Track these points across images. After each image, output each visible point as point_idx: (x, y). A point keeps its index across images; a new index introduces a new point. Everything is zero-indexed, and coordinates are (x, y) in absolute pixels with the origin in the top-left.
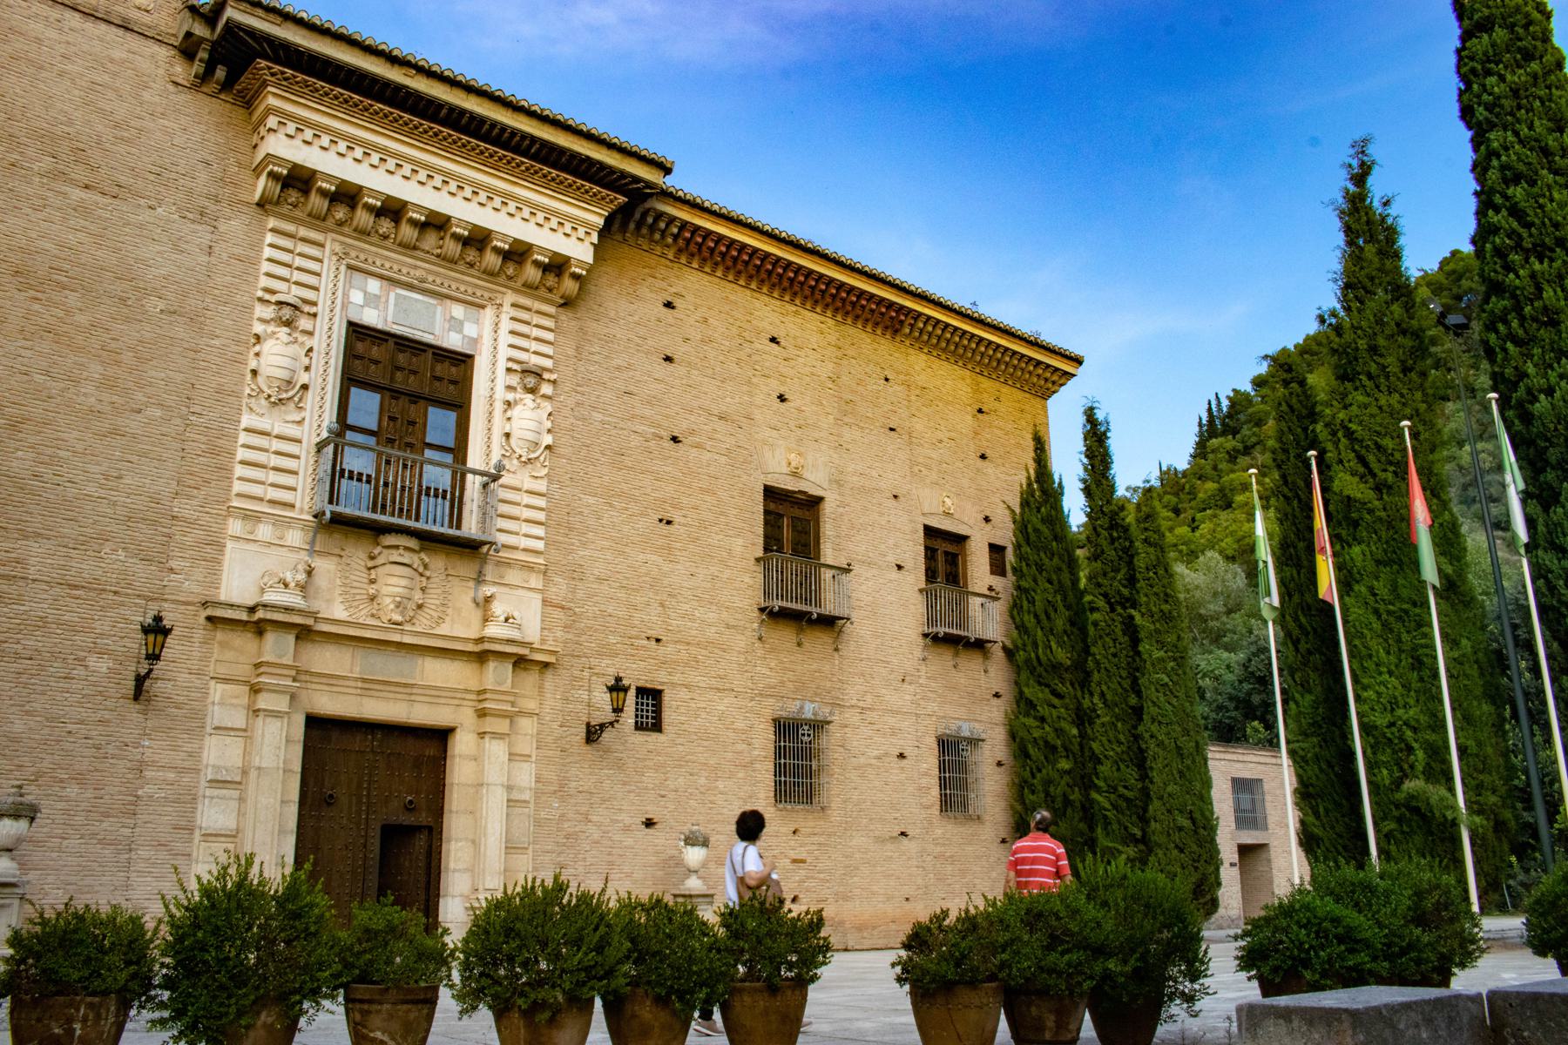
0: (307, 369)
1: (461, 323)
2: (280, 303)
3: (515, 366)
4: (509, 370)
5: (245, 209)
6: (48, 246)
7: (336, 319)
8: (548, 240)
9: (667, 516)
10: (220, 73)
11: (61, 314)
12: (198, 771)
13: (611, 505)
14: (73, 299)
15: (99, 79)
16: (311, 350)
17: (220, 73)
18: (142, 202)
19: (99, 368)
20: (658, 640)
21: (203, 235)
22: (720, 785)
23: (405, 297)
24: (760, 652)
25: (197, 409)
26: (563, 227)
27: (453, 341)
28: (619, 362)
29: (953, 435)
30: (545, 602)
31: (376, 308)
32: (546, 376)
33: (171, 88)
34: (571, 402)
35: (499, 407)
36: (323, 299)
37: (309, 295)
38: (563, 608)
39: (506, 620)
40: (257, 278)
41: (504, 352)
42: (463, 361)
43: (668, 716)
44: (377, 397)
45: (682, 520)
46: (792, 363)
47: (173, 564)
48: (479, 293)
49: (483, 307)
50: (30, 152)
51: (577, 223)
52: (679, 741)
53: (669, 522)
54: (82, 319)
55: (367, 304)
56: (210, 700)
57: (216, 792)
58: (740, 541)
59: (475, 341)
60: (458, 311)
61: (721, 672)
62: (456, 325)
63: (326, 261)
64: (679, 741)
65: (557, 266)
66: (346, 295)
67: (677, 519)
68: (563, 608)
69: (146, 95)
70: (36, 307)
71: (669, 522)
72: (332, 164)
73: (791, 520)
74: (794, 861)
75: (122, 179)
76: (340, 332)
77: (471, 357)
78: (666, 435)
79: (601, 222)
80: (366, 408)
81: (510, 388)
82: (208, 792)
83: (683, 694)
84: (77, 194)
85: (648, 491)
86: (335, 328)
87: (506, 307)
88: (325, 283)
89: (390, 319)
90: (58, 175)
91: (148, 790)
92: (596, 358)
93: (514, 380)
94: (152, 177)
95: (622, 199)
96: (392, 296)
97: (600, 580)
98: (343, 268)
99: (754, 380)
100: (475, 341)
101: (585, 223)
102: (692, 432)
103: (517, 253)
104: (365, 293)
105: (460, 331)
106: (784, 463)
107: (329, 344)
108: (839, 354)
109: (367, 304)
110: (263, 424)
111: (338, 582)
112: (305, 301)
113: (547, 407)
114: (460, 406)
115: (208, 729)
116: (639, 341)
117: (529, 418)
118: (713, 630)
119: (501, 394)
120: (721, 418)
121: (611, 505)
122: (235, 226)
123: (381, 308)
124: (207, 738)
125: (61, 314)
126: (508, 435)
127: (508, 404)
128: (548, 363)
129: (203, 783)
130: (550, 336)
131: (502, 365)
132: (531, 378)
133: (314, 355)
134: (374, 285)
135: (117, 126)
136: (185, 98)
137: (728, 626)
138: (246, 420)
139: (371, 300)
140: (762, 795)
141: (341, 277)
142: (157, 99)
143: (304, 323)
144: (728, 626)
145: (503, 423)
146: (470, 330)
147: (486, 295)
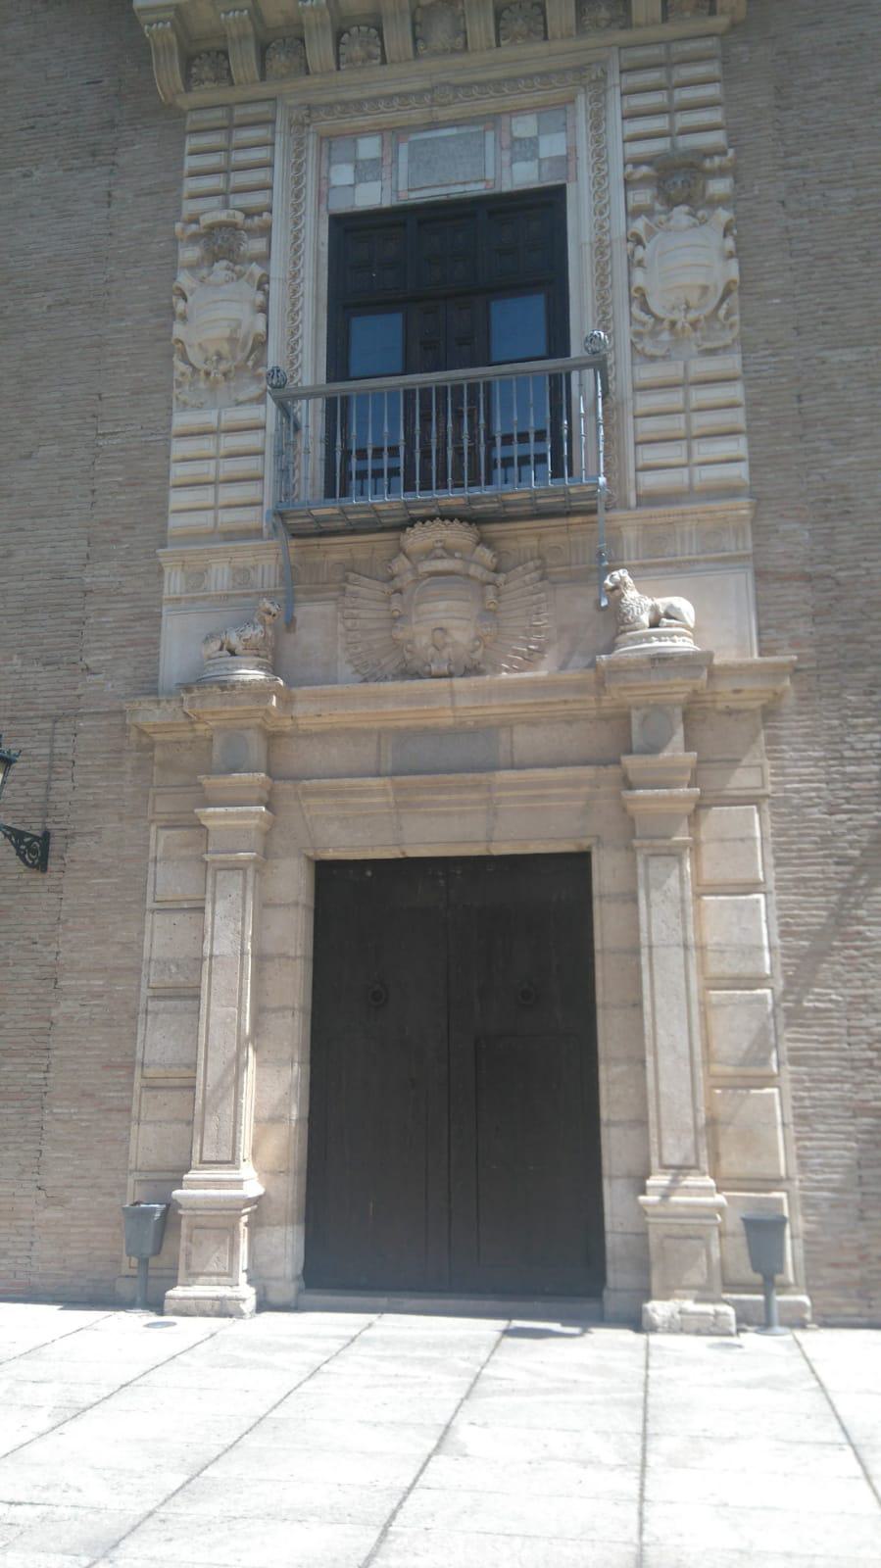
0: (264, 309)
1: (533, 142)
4: (628, 183)
7: (309, 221)
12: (137, 971)
16: (263, 284)
18: (14, 173)
23: (425, 142)
25: (108, 428)
27: (523, 176)
30: (760, 575)
31: (378, 178)
35: (620, 252)
36: (279, 199)
38: (808, 578)
39: (654, 624)
41: (617, 152)
42: (546, 206)
44: (396, 320)
47: (89, 661)
56: (152, 855)
57: (162, 1004)
59: (565, 160)
60: (525, 127)
62: (526, 148)
63: (279, 140)
66: (323, 180)
68: (808, 578)
76: (316, 239)
81: (632, 214)
82: (152, 1005)
86: (308, 234)
87: (614, 78)
88: (279, 175)
89: (402, 187)
91: (67, 1006)
93: (643, 196)
98: (311, 141)
100: (567, 160)
104: (357, 164)
105: (535, 155)
110: (209, 418)
111: (340, 628)
112: (249, 214)
115: (150, 904)
119: (619, 225)
124: (149, 917)
128: (716, 138)
129: (145, 992)
130: (711, 91)
131: (617, 173)
132: (675, 180)
133: (275, 288)
138: (181, 420)
139: (365, 171)
141: (311, 155)
143: (257, 246)
146: (552, 146)
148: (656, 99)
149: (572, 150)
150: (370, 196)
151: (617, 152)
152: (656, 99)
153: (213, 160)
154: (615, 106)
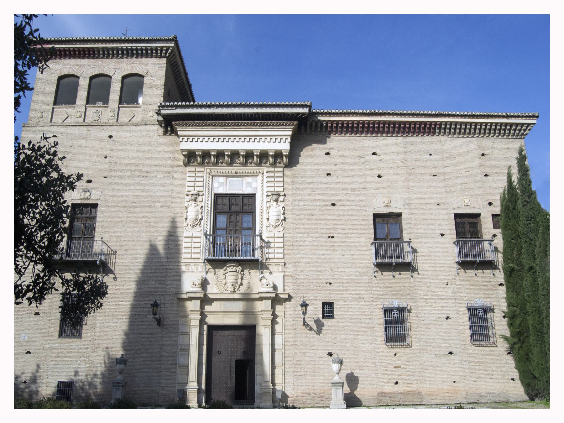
1: (251, 183)
2: (192, 194)
3: (269, 194)
5: (181, 168)
6: (131, 196)
8: (271, 147)
9: (331, 235)
10: (169, 129)
11: (135, 215)
13: (308, 235)
14: (138, 210)
15: (140, 143)
17: (169, 129)
18: (153, 175)
19: (145, 228)
20: (330, 283)
21: (170, 179)
22: (360, 337)
23: (232, 180)
24: (375, 282)
26: (278, 139)
28: (309, 181)
29: (468, 170)
32: (281, 194)
33: (159, 138)
34: (291, 201)
35: (265, 209)
37: (201, 189)
40: (185, 188)
41: (265, 189)
43: (336, 312)
45: (338, 235)
46: (383, 161)
48: (255, 171)
49: (258, 176)
50: (125, 171)
51: (281, 137)
52: (341, 321)
53: (333, 237)
54: (140, 215)
55: (220, 186)
58: (364, 239)
59: (256, 188)
60: (249, 179)
61: (358, 292)
62: (249, 185)
64: (341, 321)
65: (278, 155)
67: (335, 235)
69: (152, 143)
70: (129, 215)
71: (333, 237)
72: (199, 146)
73: (387, 225)
74: (395, 367)
75: (148, 170)
77: (255, 194)
78: (330, 204)
79: (290, 133)
80: (222, 220)
83: (342, 303)
84: (137, 179)
85: (323, 227)
90: (133, 175)
92: (299, 182)
94: (155, 167)
95: (296, 122)
96: (228, 181)
97: (306, 264)
99: (366, 172)
101: (284, 136)
102: (340, 200)
103: (263, 155)
106: (382, 203)
107: (207, 203)
108: (406, 150)
109: (220, 186)
113: (282, 205)
114: (252, 213)
116: (316, 171)
117: (275, 211)
118: (353, 276)
120: (352, 191)
121: (308, 235)
122: (178, 174)
123: (226, 185)
125: (135, 215)
126: (268, 219)
127: (267, 208)
134: (222, 179)
135: (146, 155)
136: (163, 139)
137: (360, 273)
139: (221, 185)
140: (379, 340)
142: (155, 143)
144: (360, 273)
145: (266, 215)
146: (254, 185)
147: (258, 171)
148: (272, 179)
149: (257, 186)
150: (221, 191)
151: (265, 189)
152: (272, 179)
153: (193, 179)
154: (265, 180)
